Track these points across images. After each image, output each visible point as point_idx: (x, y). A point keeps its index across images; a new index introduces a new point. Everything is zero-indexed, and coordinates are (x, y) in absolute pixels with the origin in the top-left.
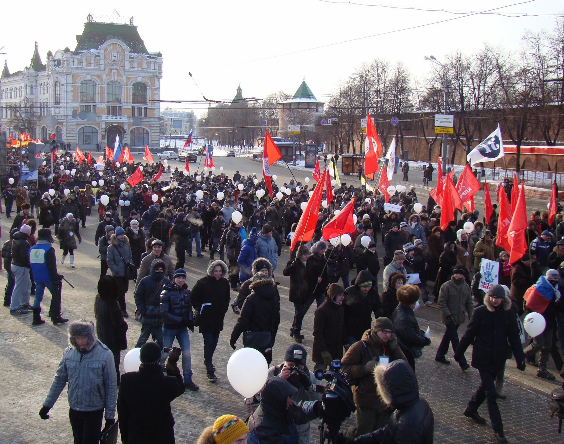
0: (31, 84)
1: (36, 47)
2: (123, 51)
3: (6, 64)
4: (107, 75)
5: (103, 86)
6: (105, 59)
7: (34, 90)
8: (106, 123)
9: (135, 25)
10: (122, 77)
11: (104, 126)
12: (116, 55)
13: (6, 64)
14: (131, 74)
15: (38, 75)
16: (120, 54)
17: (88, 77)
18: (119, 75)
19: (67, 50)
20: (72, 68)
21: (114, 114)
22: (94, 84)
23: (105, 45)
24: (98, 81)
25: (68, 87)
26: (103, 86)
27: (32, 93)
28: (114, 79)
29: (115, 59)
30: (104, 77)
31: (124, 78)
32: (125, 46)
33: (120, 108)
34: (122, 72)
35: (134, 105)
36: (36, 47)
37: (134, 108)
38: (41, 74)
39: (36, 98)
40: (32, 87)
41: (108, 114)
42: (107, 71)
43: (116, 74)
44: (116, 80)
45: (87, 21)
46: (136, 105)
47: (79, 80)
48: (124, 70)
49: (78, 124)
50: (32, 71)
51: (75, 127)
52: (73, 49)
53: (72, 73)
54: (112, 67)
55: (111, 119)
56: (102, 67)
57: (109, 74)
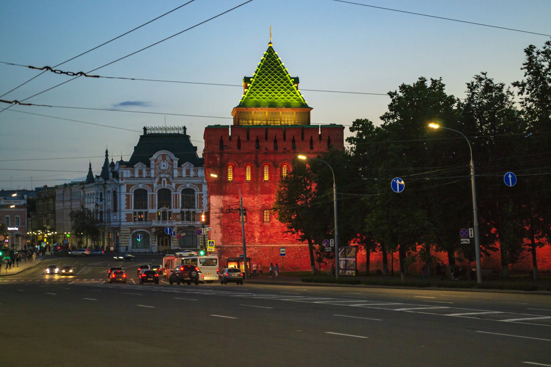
0: (99, 192)
1: (107, 155)
2: (172, 160)
3: (90, 169)
4: (158, 183)
5: (154, 193)
6: (155, 169)
7: (103, 197)
8: (156, 227)
9: (187, 134)
10: (171, 184)
11: (154, 230)
12: (165, 164)
13: (90, 169)
14: (180, 181)
15: (106, 183)
16: (169, 163)
17: (140, 186)
18: (169, 182)
19: (121, 163)
20: (127, 178)
21: (165, 219)
22: (146, 192)
23: (155, 156)
24: (149, 189)
25: (122, 196)
26: (154, 193)
27: (101, 200)
28: (164, 186)
29: (162, 168)
30: (155, 185)
31: (174, 185)
32: (173, 156)
33: (170, 213)
34: (171, 180)
35: (183, 210)
36: (107, 155)
37: (182, 213)
38: (108, 182)
39: (105, 204)
40: (101, 194)
41: (159, 219)
42: (157, 180)
43: (166, 182)
44: (166, 187)
45: (143, 134)
46: (185, 210)
47: (132, 190)
48: (173, 177)
49: (132, 229)
50: (101, 179)
51: (129, 232)
52: (127, 159)
53: (126, 183)
54: (162, 176)
55: (161, 224)
56: (153, 176)
57: (159, 182)
